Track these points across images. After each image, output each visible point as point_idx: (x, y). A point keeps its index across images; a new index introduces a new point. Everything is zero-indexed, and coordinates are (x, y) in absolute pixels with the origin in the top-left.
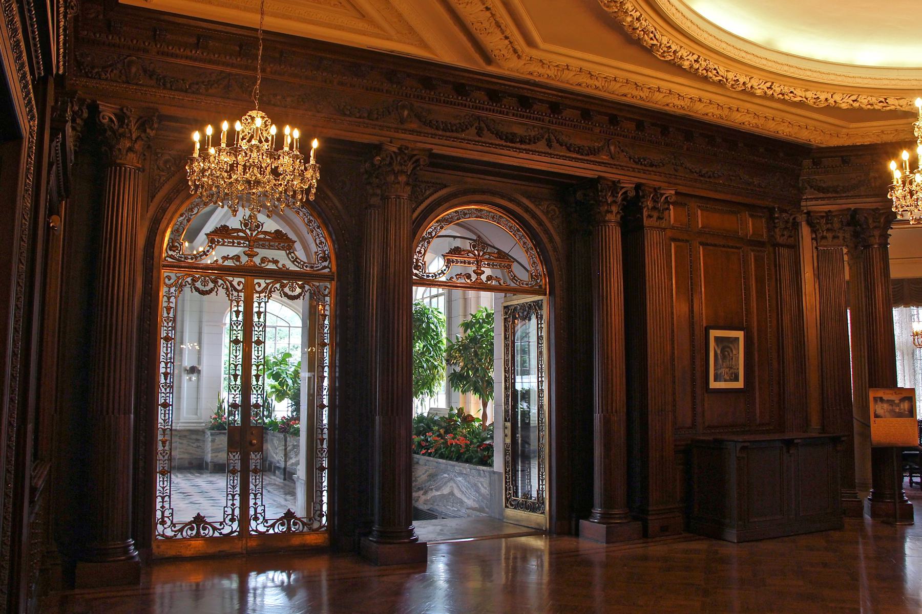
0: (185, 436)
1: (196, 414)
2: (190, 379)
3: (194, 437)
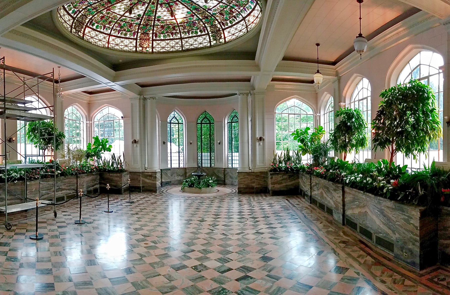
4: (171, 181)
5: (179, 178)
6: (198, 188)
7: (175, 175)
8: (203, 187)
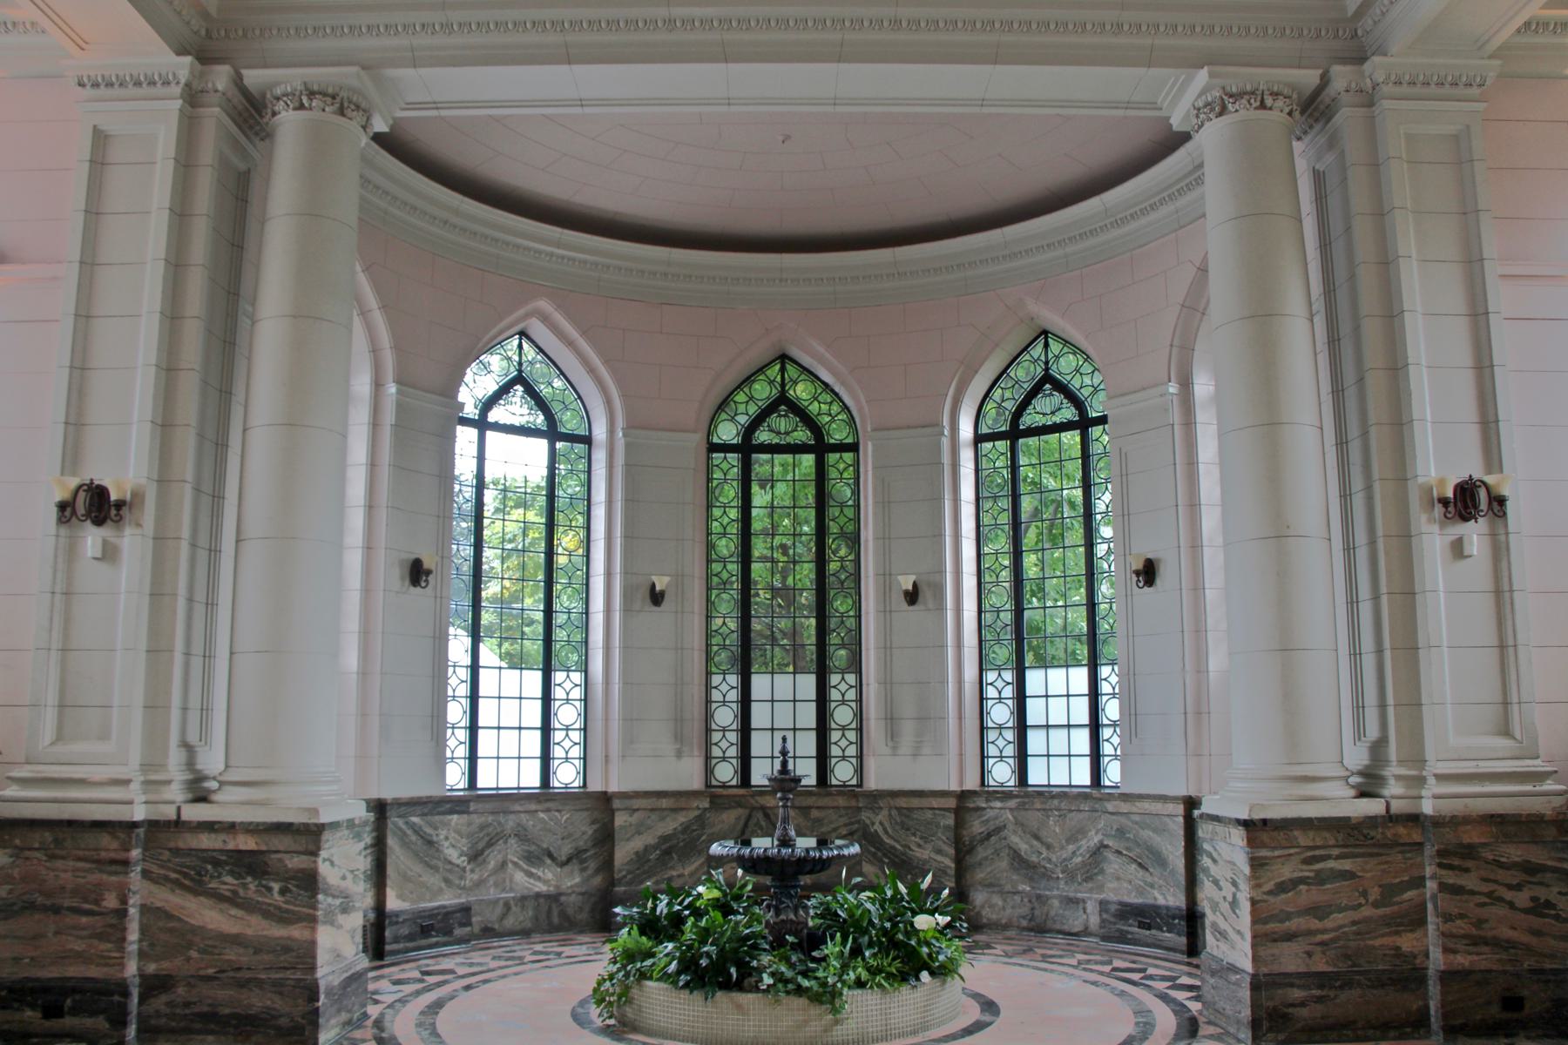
0: (1469, 851)
1: (1506, 732)
2: (1458, 549)
3: (1514, 853)
4: (466, 910)
5: (547, 879)
6: (800, 991)
7: (512, 850)
8: (860, 984)
